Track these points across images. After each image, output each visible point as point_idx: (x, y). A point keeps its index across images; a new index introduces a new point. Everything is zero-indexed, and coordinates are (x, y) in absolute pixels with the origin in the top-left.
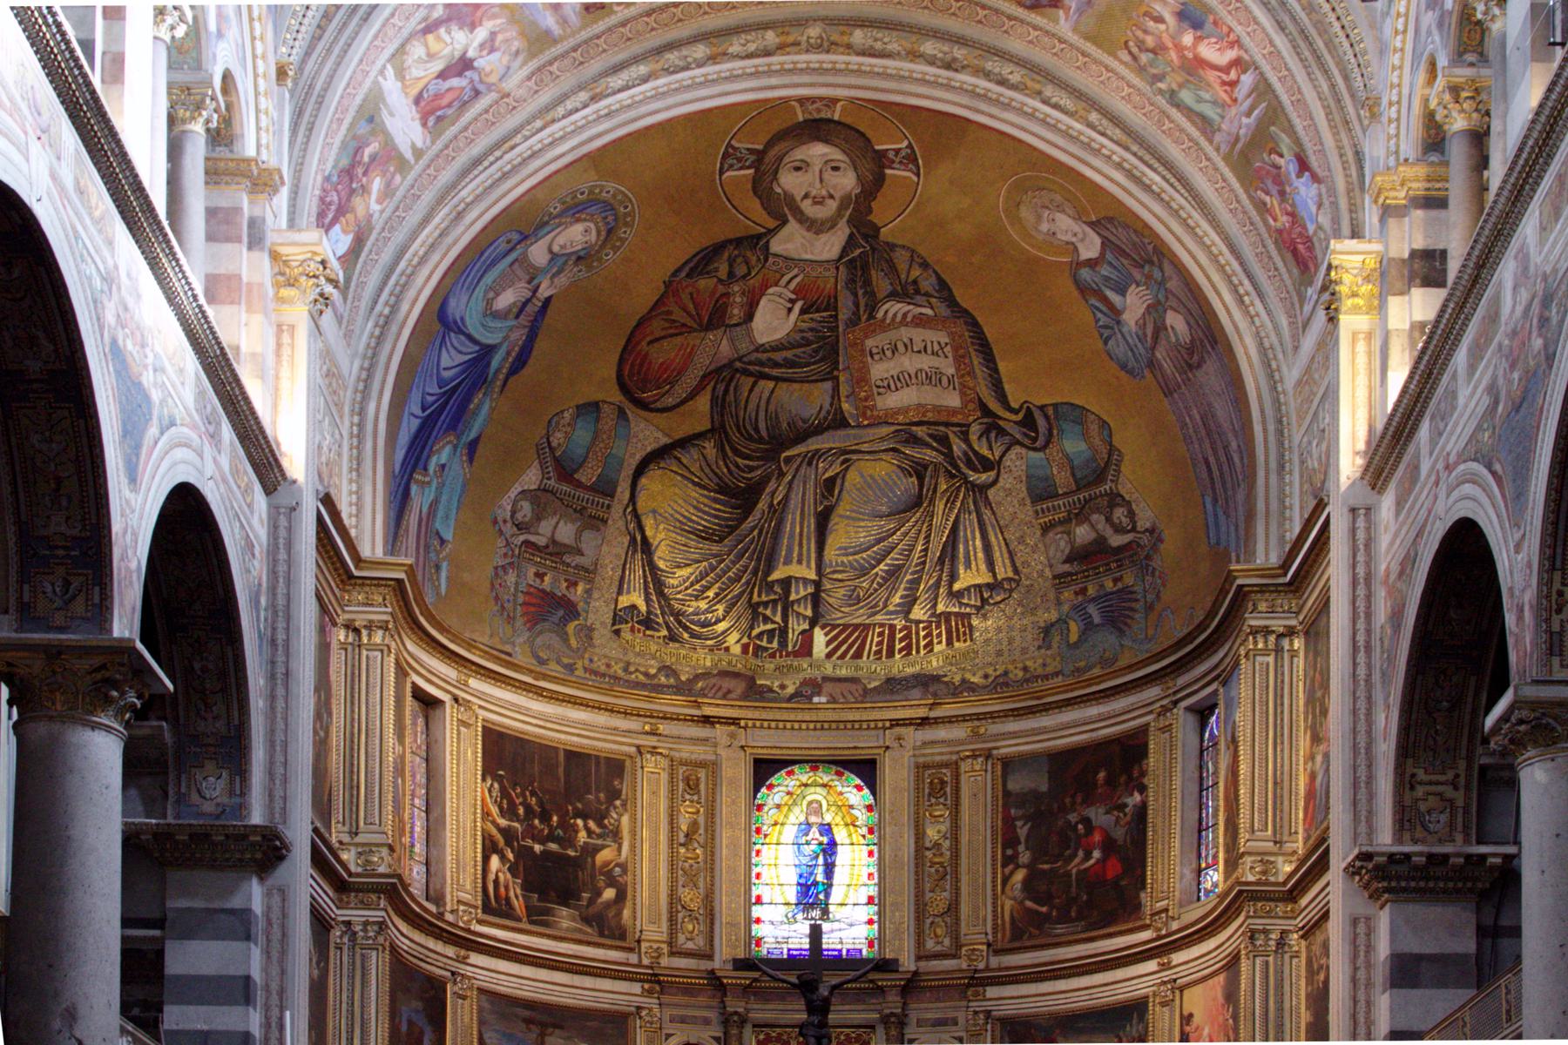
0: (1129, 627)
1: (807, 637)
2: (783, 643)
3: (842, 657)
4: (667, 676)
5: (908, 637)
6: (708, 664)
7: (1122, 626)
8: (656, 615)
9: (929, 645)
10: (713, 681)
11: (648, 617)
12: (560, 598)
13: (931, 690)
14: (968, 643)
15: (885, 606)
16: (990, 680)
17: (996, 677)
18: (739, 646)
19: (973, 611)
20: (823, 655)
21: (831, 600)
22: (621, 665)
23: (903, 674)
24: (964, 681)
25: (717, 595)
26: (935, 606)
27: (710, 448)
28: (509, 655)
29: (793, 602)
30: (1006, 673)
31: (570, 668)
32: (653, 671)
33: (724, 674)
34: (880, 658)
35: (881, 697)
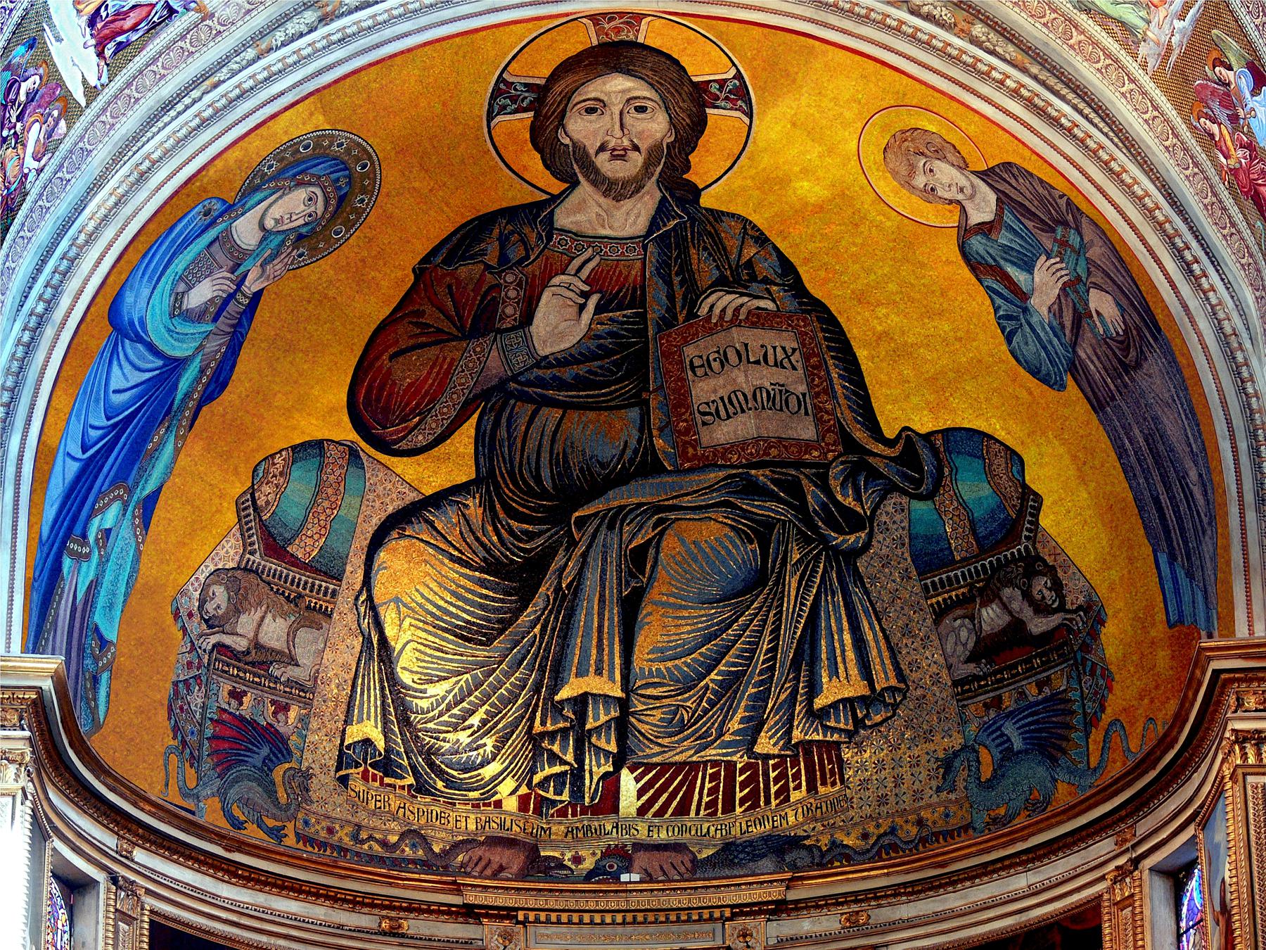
0: (1064, 752)
1: (611, 783)
2: (577, 793)
3: (660, 813)
4: (414, 846)
5: (752, 779)
6: (472, 827)
7: (1055, 752)
8: (398, 754)
9: (784, 792)
10: (479, 852)
11: (387, 757)
12: (264, 729)
13: (788, 858)
14: (838, 787)
15: (720, 735)
16: (871, 841)
17: (880, 837)
18: (514, 799)
19: (843, 738)
20: (633, 811)
21: (643, 728)
22: (348, 829)
23: (746, 837)
24: (834, 844)
25: (484, 722)
26: (789, 732)
27: (474, 508)
28: (193, 813)
29: (590, 730)
30: (893, 830)
31: (277, 833)
32: (393, 839)
33: (494, 842)
34: (715, 813)
35: (718, 872)
